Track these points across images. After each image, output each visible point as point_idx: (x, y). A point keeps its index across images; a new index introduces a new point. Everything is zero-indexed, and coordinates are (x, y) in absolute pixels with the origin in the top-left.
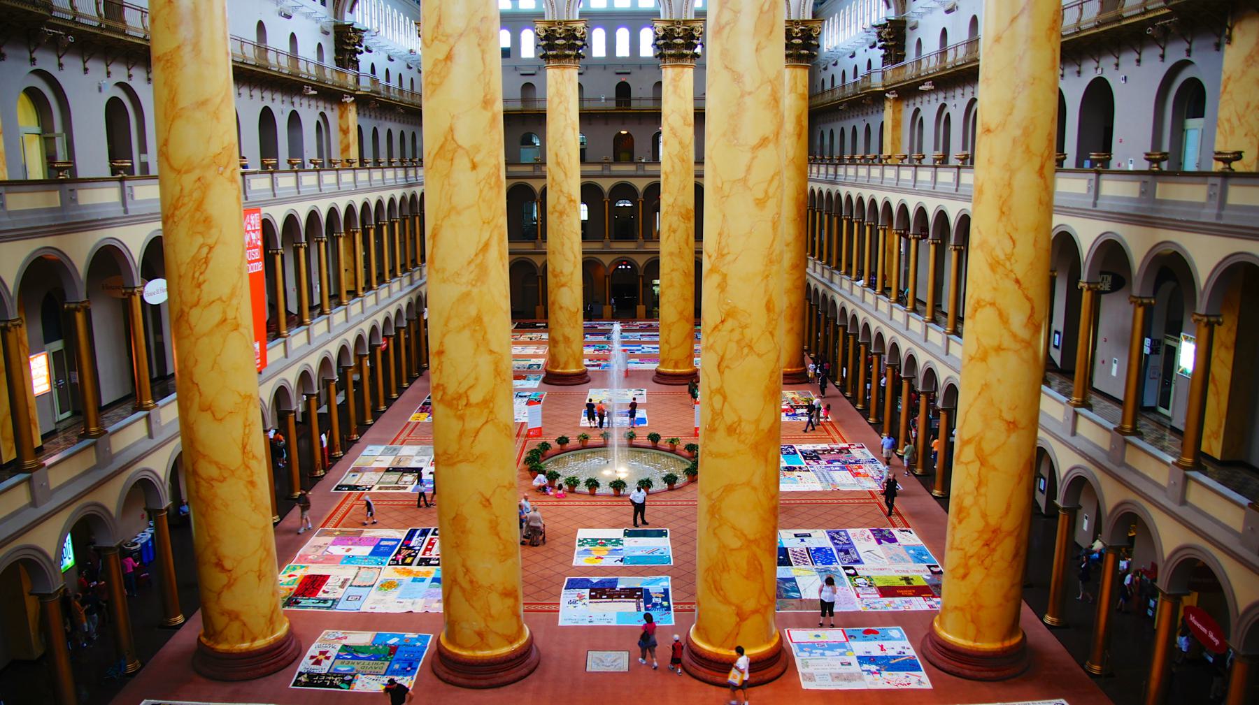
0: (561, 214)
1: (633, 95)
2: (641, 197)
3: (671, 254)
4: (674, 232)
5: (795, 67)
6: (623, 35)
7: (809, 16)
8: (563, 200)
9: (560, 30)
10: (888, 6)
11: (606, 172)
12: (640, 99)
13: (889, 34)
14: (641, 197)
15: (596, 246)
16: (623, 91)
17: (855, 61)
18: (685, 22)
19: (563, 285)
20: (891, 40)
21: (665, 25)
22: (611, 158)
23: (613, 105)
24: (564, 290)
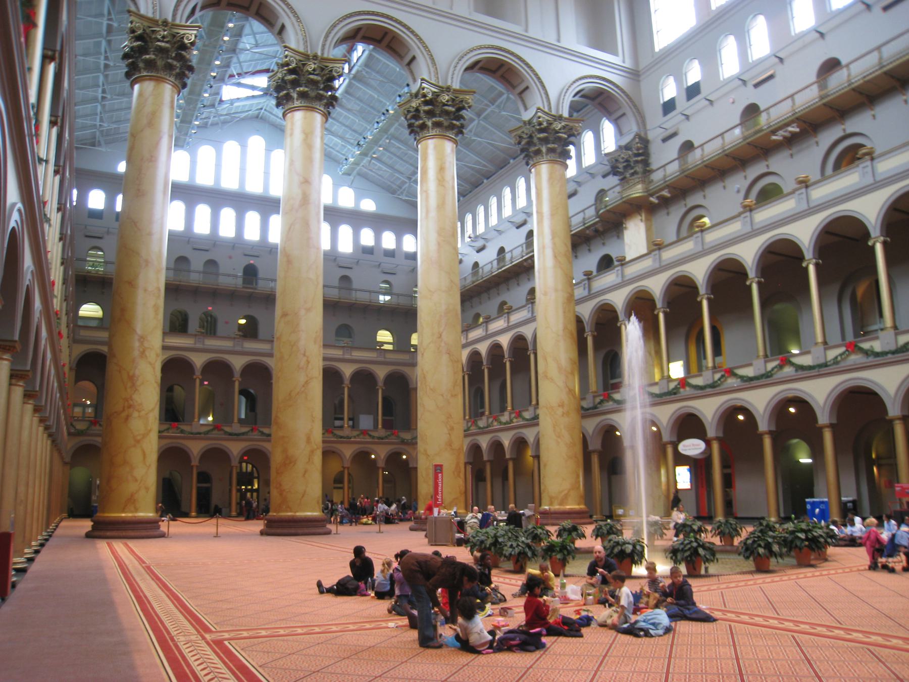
1: (261, 274)
11: (238, 348)
13: (638, 149)
17: (524, 230)
23: (240, 281)
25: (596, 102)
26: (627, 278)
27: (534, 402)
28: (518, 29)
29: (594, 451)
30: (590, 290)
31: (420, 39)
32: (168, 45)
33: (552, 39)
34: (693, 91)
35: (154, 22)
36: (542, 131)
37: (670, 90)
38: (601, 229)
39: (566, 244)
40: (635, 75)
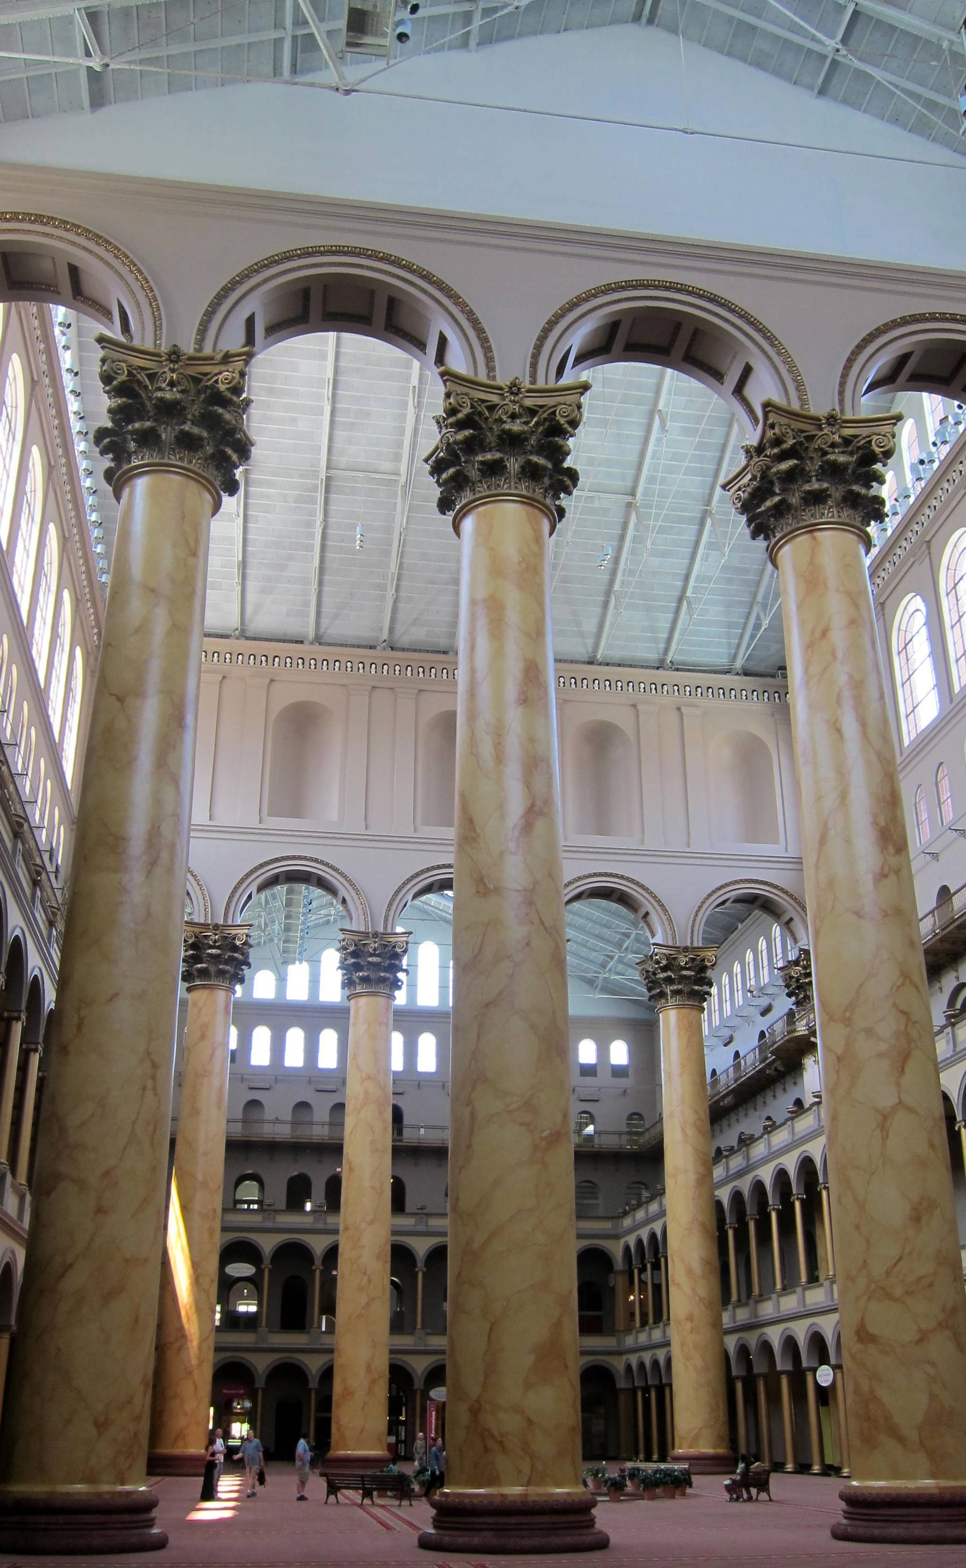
2: (420, 1264)
9: (372, 945)
10: (795, 940)
14: (420, 1264)
17: (731, 1049)
26: (775, 1149)
27: (665, 1318)
28: (630, 843)
29: (738, 1378)
32: (219, 951)
35: (205, 925)
36: (664, 969)
38: (781, 1068)
39: (696, 1112)
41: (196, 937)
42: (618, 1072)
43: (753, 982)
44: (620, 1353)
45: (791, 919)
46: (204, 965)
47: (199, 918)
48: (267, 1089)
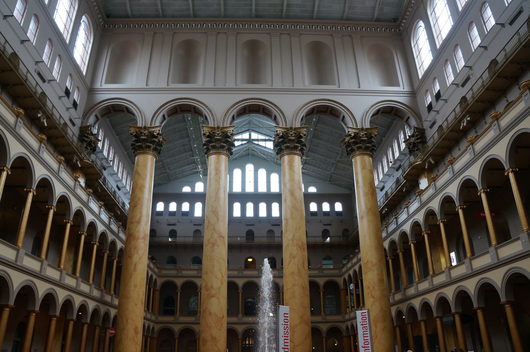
0: (213, 245)
1: (255, 235)
3: (293, 273)
4: (294, 257)
5: (364, 154)
6: (250, 206)
7: (368, 126)
8: (215, 236)
11: (241, 275)
12: (260, 237)
13: (417, 136)
15: (234, 319)
16: (250, 234)
18: (295, 129)
19: (212, 297)
20: (418, 139)
21: (283, 130)
22: (243, 267)
23: (244, 240)
24: (214, 300)
25: (389, 116)
30: (397, 224)
31: (275, 106)
32: (146, 137)
33: (356, 88)
34: (438, 96)
37: (429, 99)
40: (413, 94)
41: (136, 132)
42: (338, 213)
43: (392, 158)
44: (344, 322)
45: (409, 118)
46: (140, 144)
47: (139, 124)
48: (200, 225)
